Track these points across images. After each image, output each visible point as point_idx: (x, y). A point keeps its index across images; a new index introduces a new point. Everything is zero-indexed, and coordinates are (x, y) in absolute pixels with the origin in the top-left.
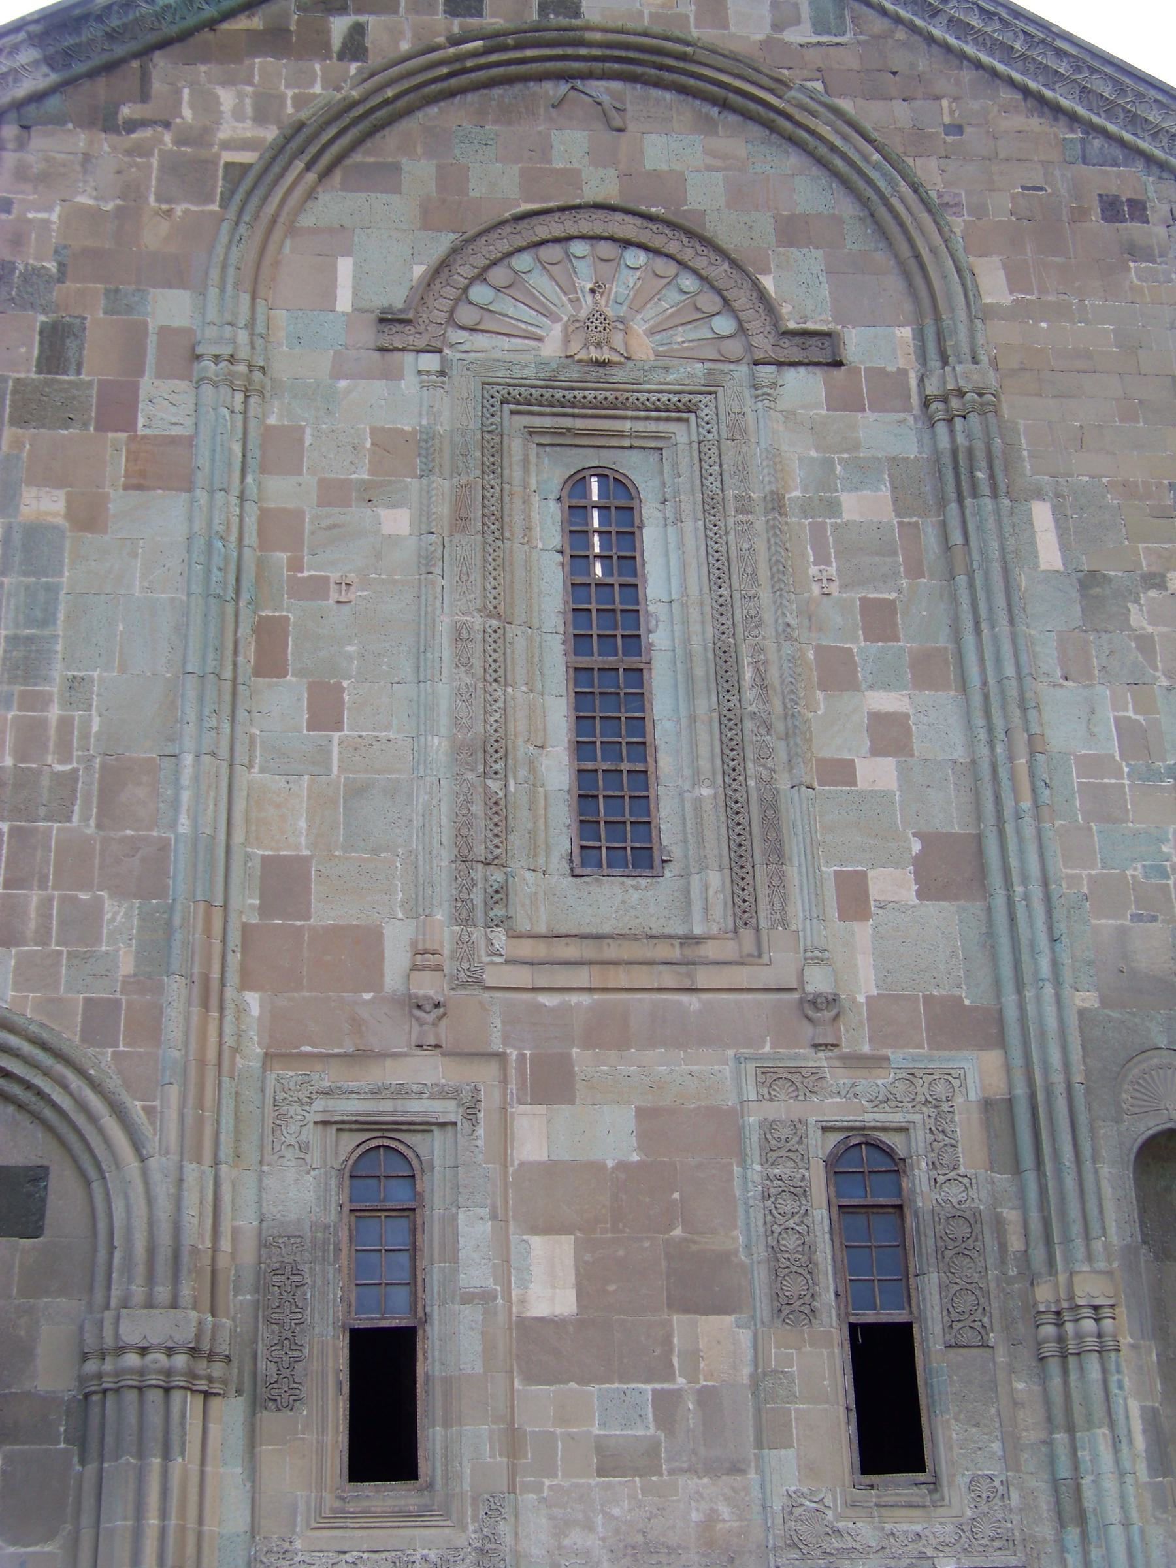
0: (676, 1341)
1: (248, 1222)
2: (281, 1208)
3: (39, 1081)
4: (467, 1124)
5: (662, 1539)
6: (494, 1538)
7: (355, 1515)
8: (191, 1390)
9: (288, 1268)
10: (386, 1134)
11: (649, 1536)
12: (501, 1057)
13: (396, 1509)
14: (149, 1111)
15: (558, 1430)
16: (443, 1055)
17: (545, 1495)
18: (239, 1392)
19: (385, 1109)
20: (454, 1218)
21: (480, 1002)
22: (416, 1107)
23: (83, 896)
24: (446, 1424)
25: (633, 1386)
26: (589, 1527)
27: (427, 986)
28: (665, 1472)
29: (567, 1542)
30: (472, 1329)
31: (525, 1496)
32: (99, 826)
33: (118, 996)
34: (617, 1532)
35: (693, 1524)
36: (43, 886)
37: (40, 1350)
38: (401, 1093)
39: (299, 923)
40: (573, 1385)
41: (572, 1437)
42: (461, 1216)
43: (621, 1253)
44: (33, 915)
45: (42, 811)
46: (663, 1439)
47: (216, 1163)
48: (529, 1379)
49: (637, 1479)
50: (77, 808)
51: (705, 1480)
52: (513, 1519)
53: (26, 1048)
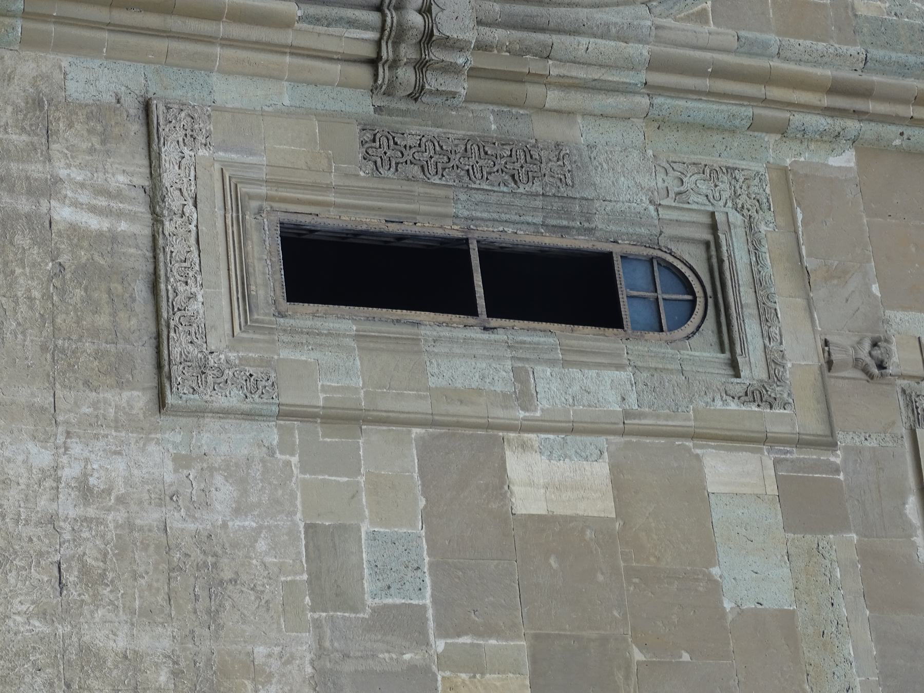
0: (493, 642)
2: (605, 166)
4: (739, 390)
5: (228, 604)
6: (221, 383)
7: (240, 222)
8: (381, 39)
9: (535, 168)
10: (710, 301)
11: (230, 587)
12: (832, 445)
13: (251, 270)
15: (362, 480)
16: (821, 367)
17: (278, 455)
18: (378, 110)
20: (619, 367)
21: (894, 423)
24: (358, 337)
25: (428, 581)
26: (238, 511)
28: (316, 615)
29: (219, 479)
30: (483, 378)
31: (275, 431)
34: (235, 545)
35: (249, 648)
38: (766, 315)
40: (422, 503)
41: (355, 495)
42: (624, 375)
43: (600, 578)
46: (361, 615)
47: (651, 89)
48: (424, 447)
49: (305, 577)
51: (309, 670)
52: (245, 407)
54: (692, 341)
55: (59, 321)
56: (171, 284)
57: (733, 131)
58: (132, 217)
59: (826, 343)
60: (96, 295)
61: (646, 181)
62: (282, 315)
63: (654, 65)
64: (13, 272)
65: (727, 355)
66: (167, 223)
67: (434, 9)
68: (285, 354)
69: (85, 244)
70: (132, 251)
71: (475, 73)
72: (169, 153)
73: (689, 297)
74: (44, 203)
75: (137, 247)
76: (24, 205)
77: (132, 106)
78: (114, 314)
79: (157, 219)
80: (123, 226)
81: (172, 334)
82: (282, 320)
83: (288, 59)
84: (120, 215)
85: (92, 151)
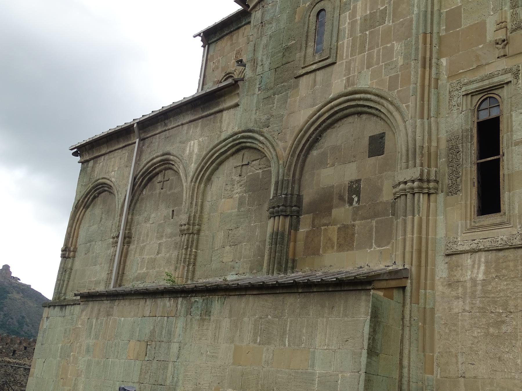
1: (443, 136)
2: (452, 127)
3: (378, 107)
4: (515, 80)
7: (478, 227)
8: (422, 193)
10: (489, 92)
13: (492, 223)
14: (407, 107)
16: (506, 58)
18: (442, 192)
19: (486, 83)
20: (511, 116)
22: (496, 80)
23: (388, 45)
24: (509, 191)
27: (501, 35)
30: (518, 155)
32: (393, 22)
33: (398, 73)
36: (378, 47)
37: (384, 189)
38: (492, 76)
39: (458, 29)
42: (514, 114)
44: (375, 56)
45: (377, 24)
47: (429, 117)
50: (387, 19)
53: (373, 97)
54: (501, 96)
55: (513, 276)
56: (498, 245)
57: (438, 93)
58: (480, 258)
59: (498, 58)
60: (504, 266)
61: (455, 115)
62: (505, 213)
63: (422, 118)
64: (499, 290)
65: (505, 85)
66: (481, 248)
67: (412, 179)
68: (516, 211)
69: (489, 270)
70: (490, 257)
71: (429, 166)
72: (460, 248)
73: (488, 99)
74: (478, 282)
75: (488, 256)
76: (479, 288)
77: (448, 259)
78: (509, 261)
79: (480, 250)
80: (483, 260)
81: (514, 244)
82: (506, 213)
83: (430, 218)
84: (480, 261)
85: (462, 270)
